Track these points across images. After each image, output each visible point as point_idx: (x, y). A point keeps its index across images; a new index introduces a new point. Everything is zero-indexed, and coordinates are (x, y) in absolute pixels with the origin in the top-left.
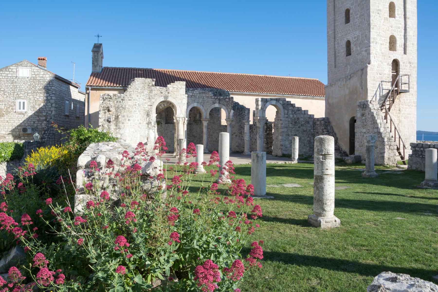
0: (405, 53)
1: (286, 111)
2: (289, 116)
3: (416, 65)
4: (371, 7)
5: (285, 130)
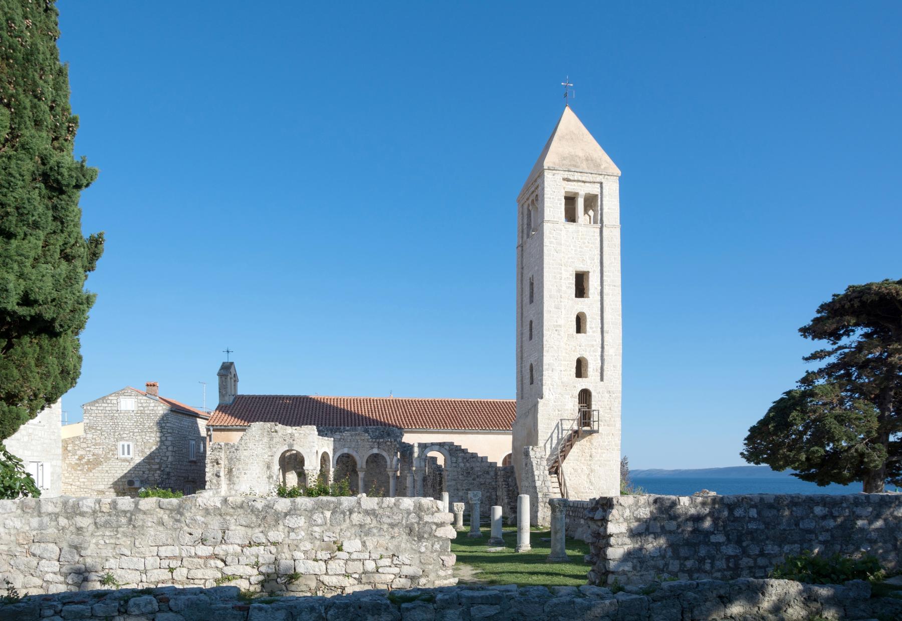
0: (602, 379)
3: (620, 395)
4: (545, 323)
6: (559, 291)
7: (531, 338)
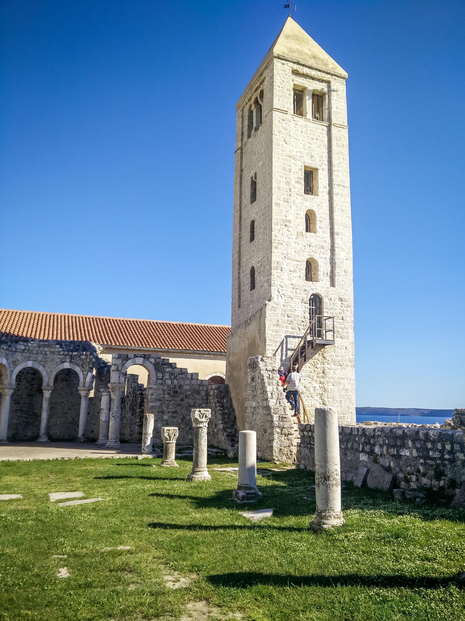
1: (160, 375)
2: (165, 381)
3: (352, 304)
4: (274, 216)
5: (158, 404)
6: (288, 183)
7: (252, 238)
